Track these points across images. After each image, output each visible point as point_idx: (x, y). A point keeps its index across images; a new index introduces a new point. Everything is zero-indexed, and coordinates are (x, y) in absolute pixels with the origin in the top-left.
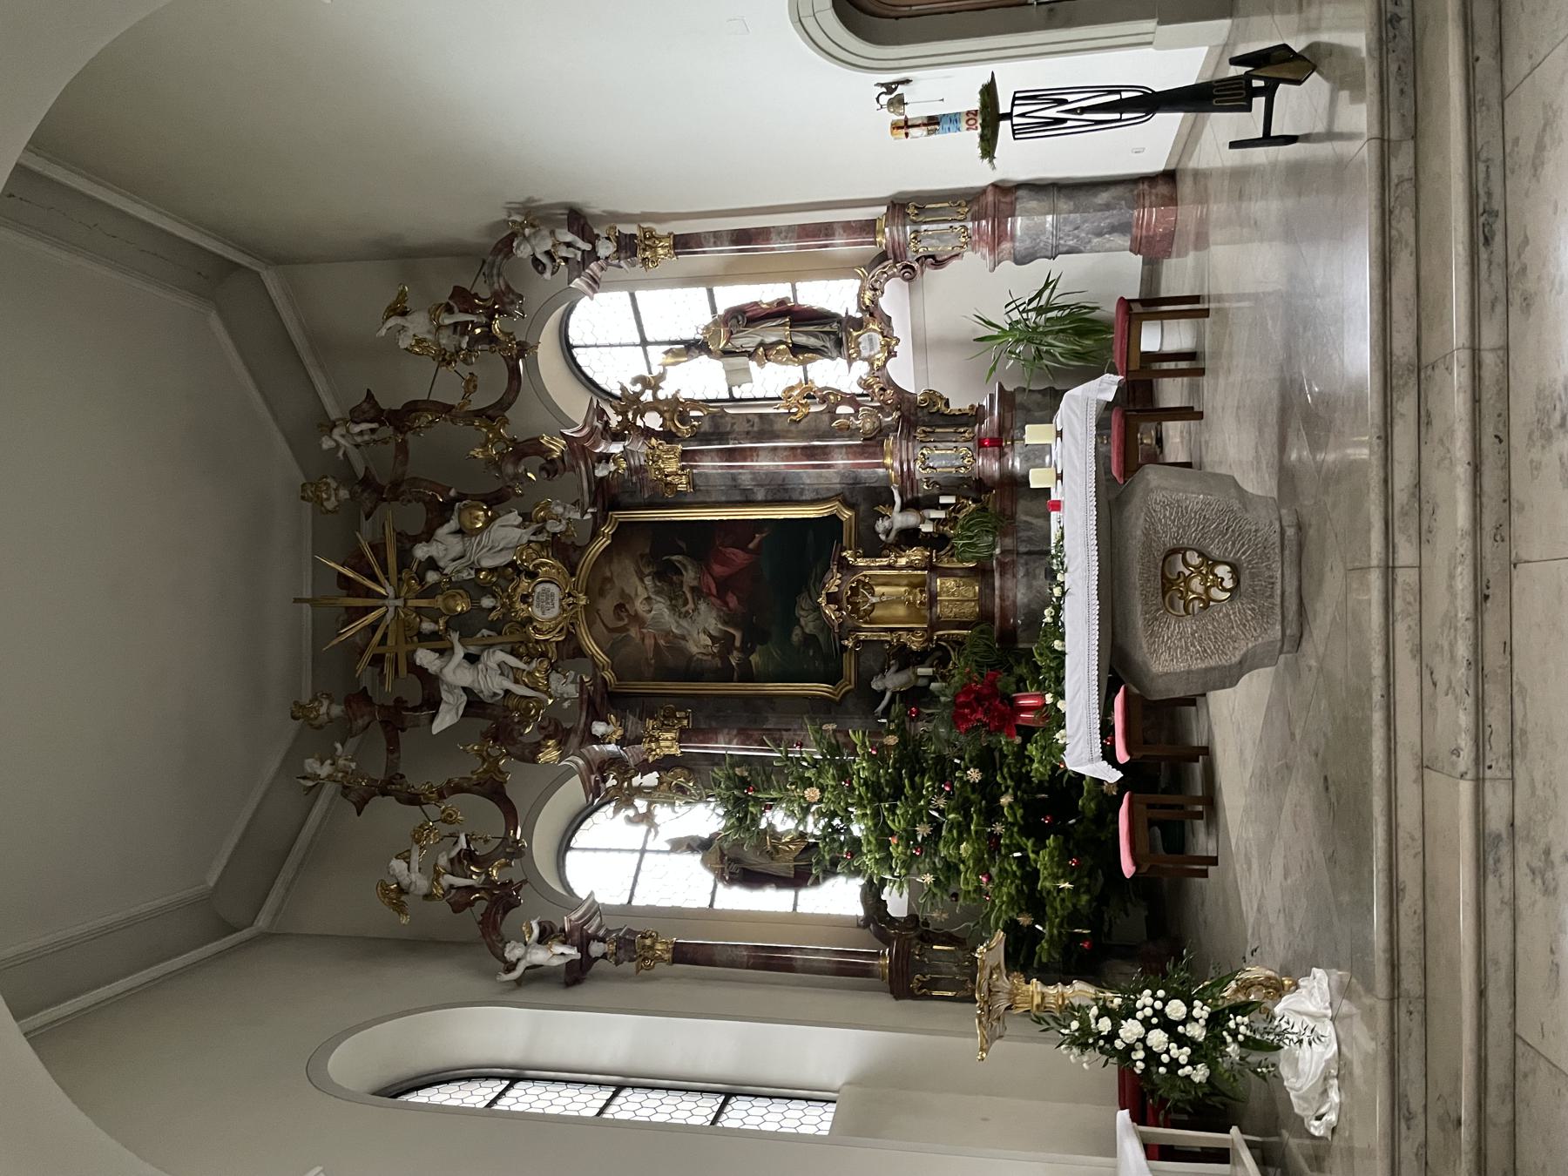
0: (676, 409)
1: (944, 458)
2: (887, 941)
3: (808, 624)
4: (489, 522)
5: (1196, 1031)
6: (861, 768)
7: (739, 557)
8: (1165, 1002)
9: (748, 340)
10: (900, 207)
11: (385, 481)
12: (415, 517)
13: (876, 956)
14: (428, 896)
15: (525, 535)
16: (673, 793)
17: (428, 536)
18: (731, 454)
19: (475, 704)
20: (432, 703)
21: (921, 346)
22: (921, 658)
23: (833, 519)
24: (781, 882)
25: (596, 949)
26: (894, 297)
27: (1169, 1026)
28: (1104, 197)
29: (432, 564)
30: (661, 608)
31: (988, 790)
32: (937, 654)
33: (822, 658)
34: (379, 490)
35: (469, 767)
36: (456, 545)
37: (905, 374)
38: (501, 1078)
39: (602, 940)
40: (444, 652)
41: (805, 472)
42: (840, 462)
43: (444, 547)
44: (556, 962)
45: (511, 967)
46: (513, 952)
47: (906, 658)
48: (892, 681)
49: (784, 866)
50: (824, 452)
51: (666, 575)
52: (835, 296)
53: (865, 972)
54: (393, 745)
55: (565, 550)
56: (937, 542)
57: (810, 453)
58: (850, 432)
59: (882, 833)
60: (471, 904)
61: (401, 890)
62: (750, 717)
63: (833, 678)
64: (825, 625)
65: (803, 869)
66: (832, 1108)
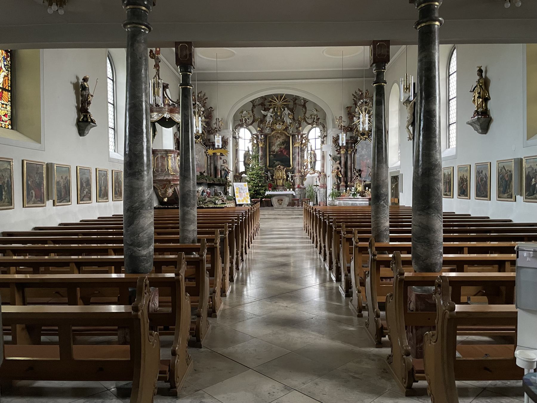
0: (306, 145)
1: (298, 181)
3: (277, 163)
4: (290, 118)
6: (260, 172)
7: (285, 154)
9: (312, 156)
10: (325, 175)
11: (296, 101)
12: (291, 106)
15: (288, 124)
16: (253, 145)
17: (288, 109)
18: (298, 153)
19: (265, 116)
20: (265, 110)
21: (313, 177)
22: (272, 178)
23: (290, 166)
24: (244, 162)
26: (316, 175)
28: (325, 198)
29: (284, 110)
30: (279, 143)
31: (259, 186)
32: (273, 180)
33: (272, 165)
34: (295, 101)
35: (257, 116)
36: (287, 113)
37: (308, 175)
40: (272, 113)
41: (296, 163)
42: (297, 168)
43: (287, 111)
47: (272, 176)
48: (269, 174)
49: (246, 161)
50: (298, 166)
51: (283, 143)
52: (318, 167)
53: (236, 172)
54: (259, 105)
55: (286, 129)
56: (287, 180)
57: (298, 164)
58: (301, 169)
59: (253, 174)
61: (242, 112)
62: (265, 155)
63: (269, 166)
64: (276, 166)
65: (245, 164)
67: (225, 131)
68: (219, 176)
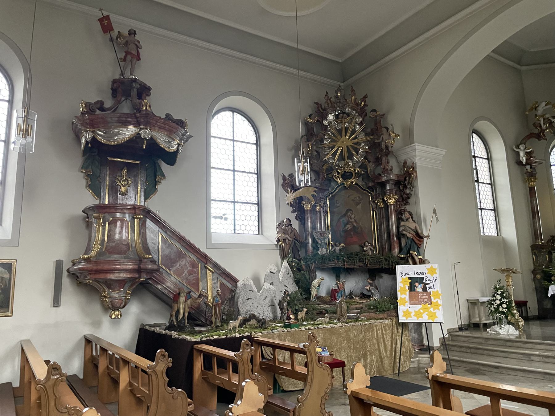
2: (548, 242)
5: (501, 309)
8: (506, 304)
13: (542, 240)
14: (536, 115)
25: (528, 167)
27: (501, 304)
38: (488, 156)
39: (531, 168)
44: (521, 159)
45: (518, 147)
46: (522, 147)
60: (536, 128)
61: (536, 108)
66: (496, 235)
67: (408, 149)
68: (396, 251)
